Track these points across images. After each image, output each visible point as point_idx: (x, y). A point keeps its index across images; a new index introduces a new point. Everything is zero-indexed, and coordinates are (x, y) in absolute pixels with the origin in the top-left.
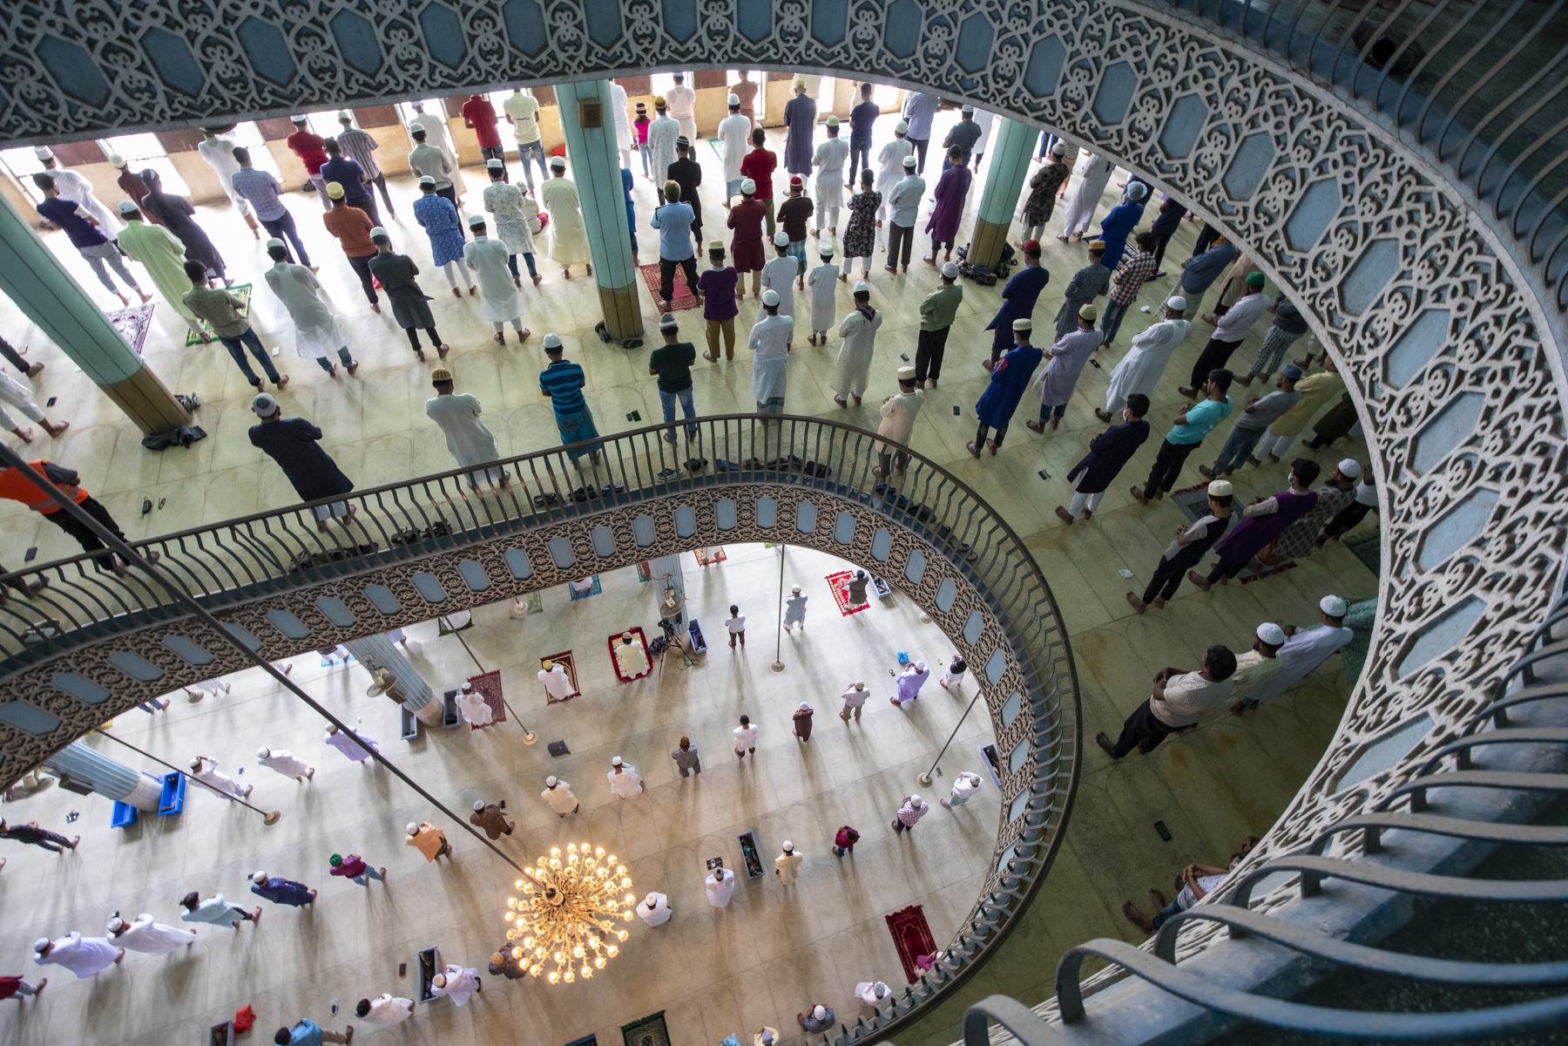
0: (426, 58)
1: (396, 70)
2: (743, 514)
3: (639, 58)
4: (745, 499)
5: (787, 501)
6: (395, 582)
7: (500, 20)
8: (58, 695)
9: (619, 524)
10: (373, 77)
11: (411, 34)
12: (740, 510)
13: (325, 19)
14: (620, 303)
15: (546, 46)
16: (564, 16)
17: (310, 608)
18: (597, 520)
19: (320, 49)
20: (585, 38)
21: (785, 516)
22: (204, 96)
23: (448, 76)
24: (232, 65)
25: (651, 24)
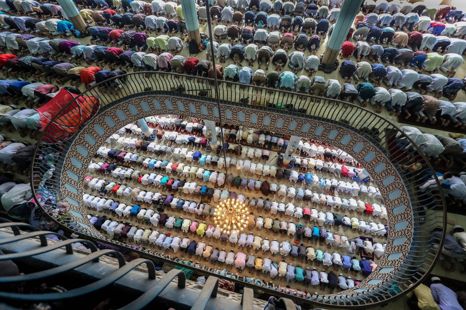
2: (338, 137)
4: (342, 133)
5: (355, 140)
6: (234, 111)
8: (152, 105)
14: (332, 55)
17: (211, 109)
21: (351, 144)
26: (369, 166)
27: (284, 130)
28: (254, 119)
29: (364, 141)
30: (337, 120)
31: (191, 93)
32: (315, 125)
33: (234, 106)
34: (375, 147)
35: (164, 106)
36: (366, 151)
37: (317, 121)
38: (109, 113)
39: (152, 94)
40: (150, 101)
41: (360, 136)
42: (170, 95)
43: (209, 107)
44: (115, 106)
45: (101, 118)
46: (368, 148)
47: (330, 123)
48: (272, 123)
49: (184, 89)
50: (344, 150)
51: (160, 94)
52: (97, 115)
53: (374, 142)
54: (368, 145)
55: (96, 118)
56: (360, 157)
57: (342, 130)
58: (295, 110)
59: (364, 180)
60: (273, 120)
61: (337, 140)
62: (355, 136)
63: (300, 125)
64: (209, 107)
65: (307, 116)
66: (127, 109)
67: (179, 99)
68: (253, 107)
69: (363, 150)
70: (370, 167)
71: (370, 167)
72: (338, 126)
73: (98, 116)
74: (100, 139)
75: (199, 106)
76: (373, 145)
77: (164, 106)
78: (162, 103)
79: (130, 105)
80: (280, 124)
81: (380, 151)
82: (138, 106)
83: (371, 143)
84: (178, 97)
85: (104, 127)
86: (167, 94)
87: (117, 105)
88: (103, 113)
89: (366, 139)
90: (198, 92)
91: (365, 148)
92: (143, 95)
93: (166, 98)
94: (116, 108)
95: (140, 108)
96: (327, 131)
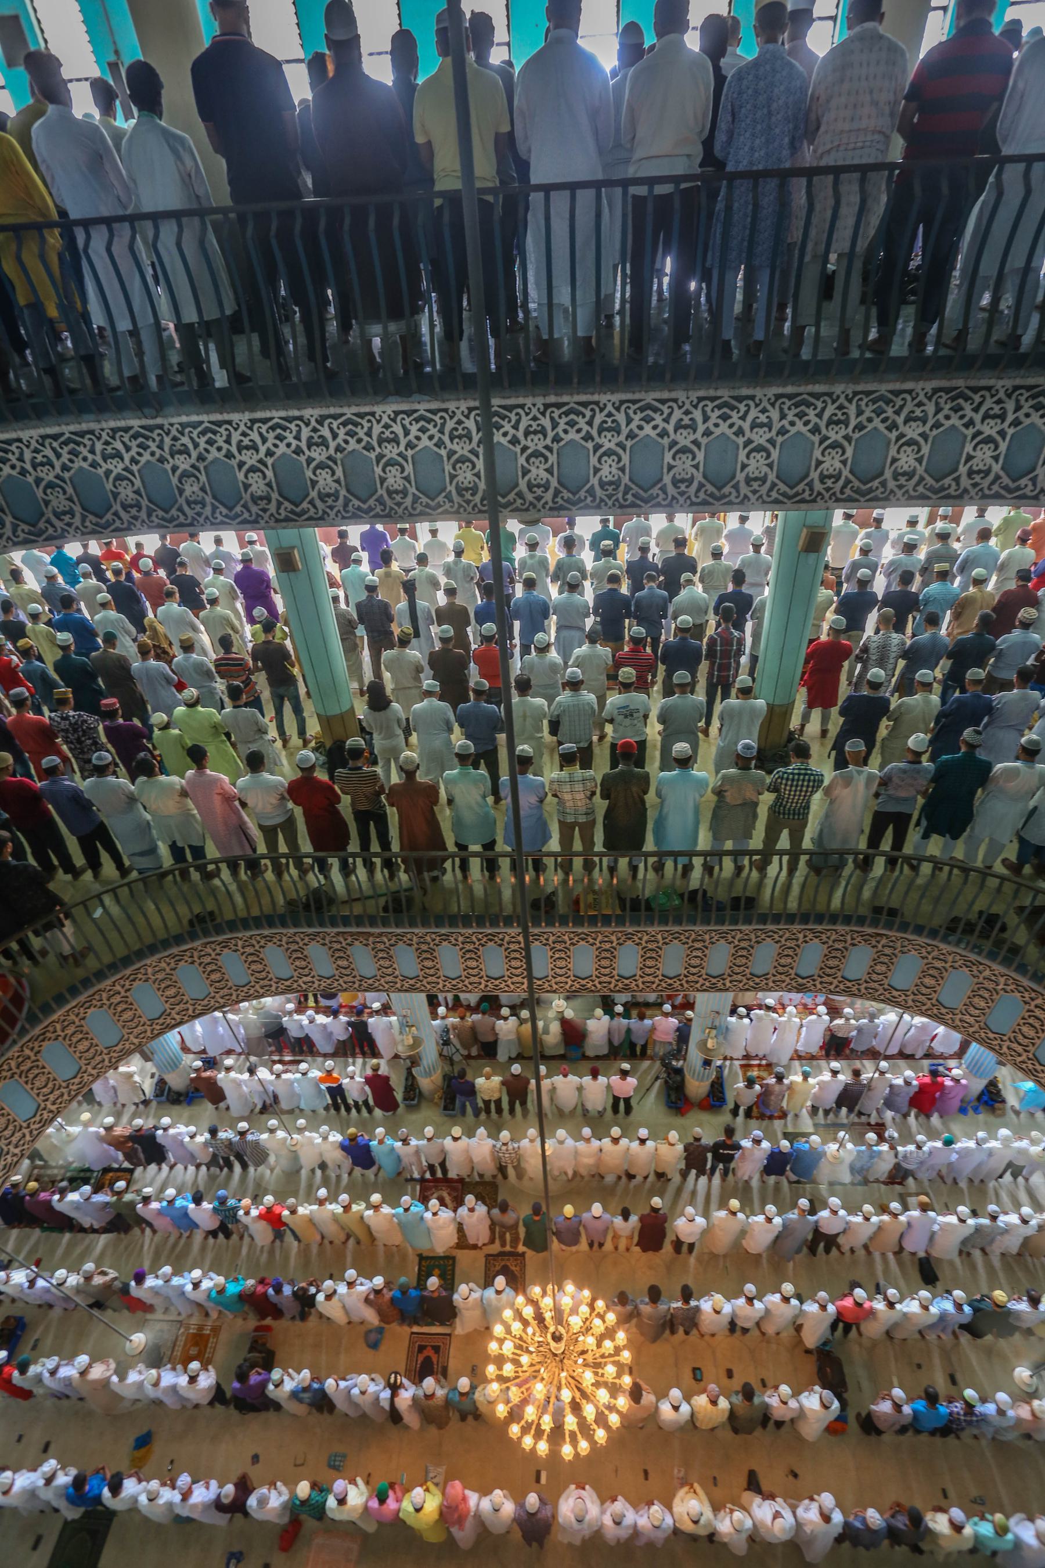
0: (772, 477)
1: (742, 485)
2: (880, 968)
3: (966, 491)
4: (887, 951)
5: (938, 964)
6: (513, 947)
7: (849, 452)
9: (743, 944)
10: (719, 489)
11: (769, 456)
12: (876, 962)
13: (704, 441)
15: (882, 474)
16: (909, 449)
17: (431, 951)
18: (723, 935)
19: (689, 462)
20: (920, 470)
21: (928, 981)
22: (582, 494)
23: (784, 495)
24: (614, 471)
25: (990, 461)
26: (1015, 1046)
27: (691, 978)
28: (584, 960)
29: (969, 964)
30: (863, 911)
31: (357, 909)
32: (792, 944)
33: (509, 931)
34: (1013, 975)
35: (260, 967)
36: (987, 995)
37: (796, 927)
38: (58, 1026)
39: (218, 934)
40: (207, 960)
41: (950, 948)
42: (284, 925)
43: (424, 947)
44: (82, 998)
45: (27, 1052)
46: (991, 986)
47: (841, 928)
48: (649, 963)
49: (331, 901)
50: (906, 1008)
51: (246, 927)
52: (15, 1042)
53: (1007, 962)
54: (987, 973)
55: (10, 1054)
56: (971, 1020)
57: (884, 941)
58: (721, 907)
59: (979, 1098)
60: (651, 954)
61: (875, 977)
62: (935, 953)
63: (743, 953)
64: (424, 947)
65: (763, 919)
66: (125, 1000)
67: (313, 937)
68: (579, 921)
69: (975, 994)
70: (1019, 1049)
71: (1019, 1049)
72: (870, 931)
73: (16, 1048)
74: (18, 1135)
75: (387, 950)
76: (1003, 970)
77: (260, 967)
78: (255, 958)
79: (136, 984)
80: (673, 960)
81: (1035, 986)
82: (167, 982)
83: (994, 966)
84: (310, 930)
85: (38, 1084)
86: (271, 925)
87: (91, 991)
88: (37, 1031)
89: (973, 957)
90: (382, 901)
91: (980, 986)
92: (185, 942)
93: (269, 939)
94: (87, 1004)
95: (171, 992)
96: (836, 954)
